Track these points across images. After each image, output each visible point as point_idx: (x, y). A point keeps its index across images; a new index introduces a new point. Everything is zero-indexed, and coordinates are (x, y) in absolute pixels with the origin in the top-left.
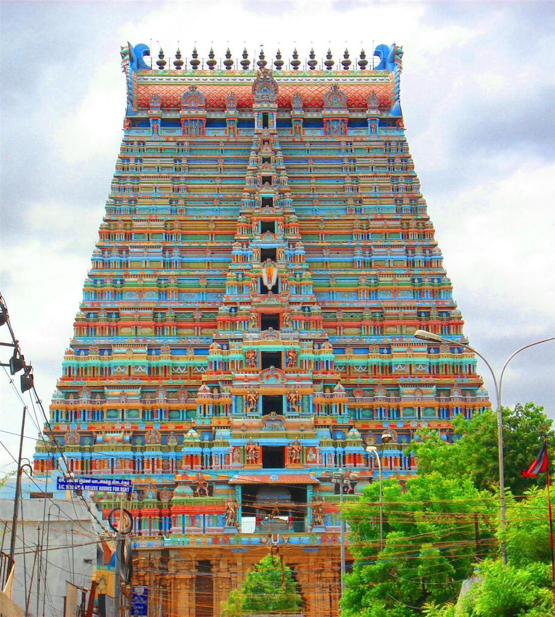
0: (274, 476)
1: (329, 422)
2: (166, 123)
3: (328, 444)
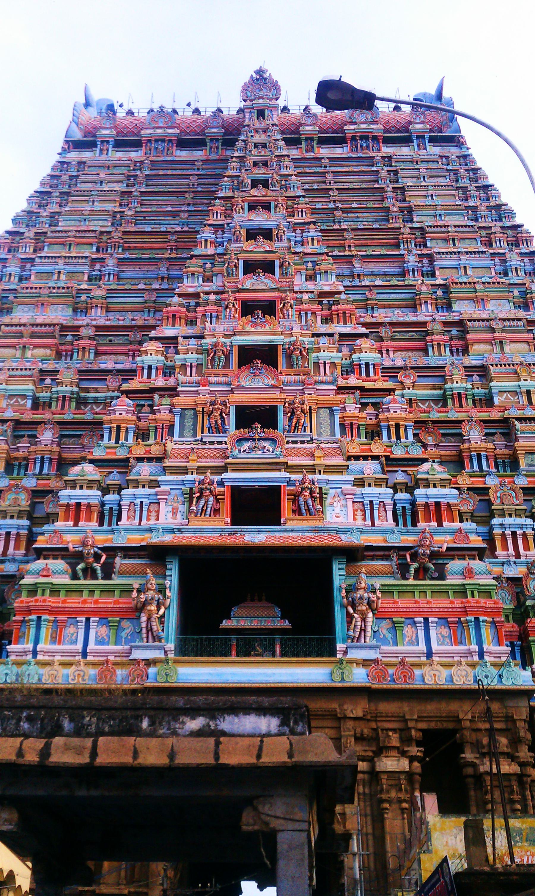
0: (257, 536)
1: (377, 449)
2: (120, 144)
3: (378, 483)
